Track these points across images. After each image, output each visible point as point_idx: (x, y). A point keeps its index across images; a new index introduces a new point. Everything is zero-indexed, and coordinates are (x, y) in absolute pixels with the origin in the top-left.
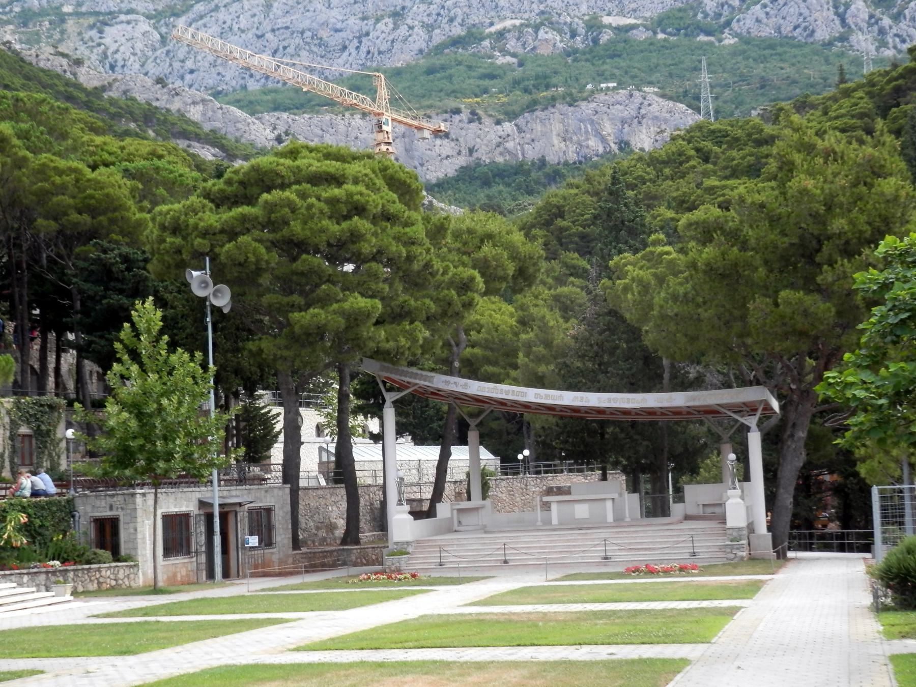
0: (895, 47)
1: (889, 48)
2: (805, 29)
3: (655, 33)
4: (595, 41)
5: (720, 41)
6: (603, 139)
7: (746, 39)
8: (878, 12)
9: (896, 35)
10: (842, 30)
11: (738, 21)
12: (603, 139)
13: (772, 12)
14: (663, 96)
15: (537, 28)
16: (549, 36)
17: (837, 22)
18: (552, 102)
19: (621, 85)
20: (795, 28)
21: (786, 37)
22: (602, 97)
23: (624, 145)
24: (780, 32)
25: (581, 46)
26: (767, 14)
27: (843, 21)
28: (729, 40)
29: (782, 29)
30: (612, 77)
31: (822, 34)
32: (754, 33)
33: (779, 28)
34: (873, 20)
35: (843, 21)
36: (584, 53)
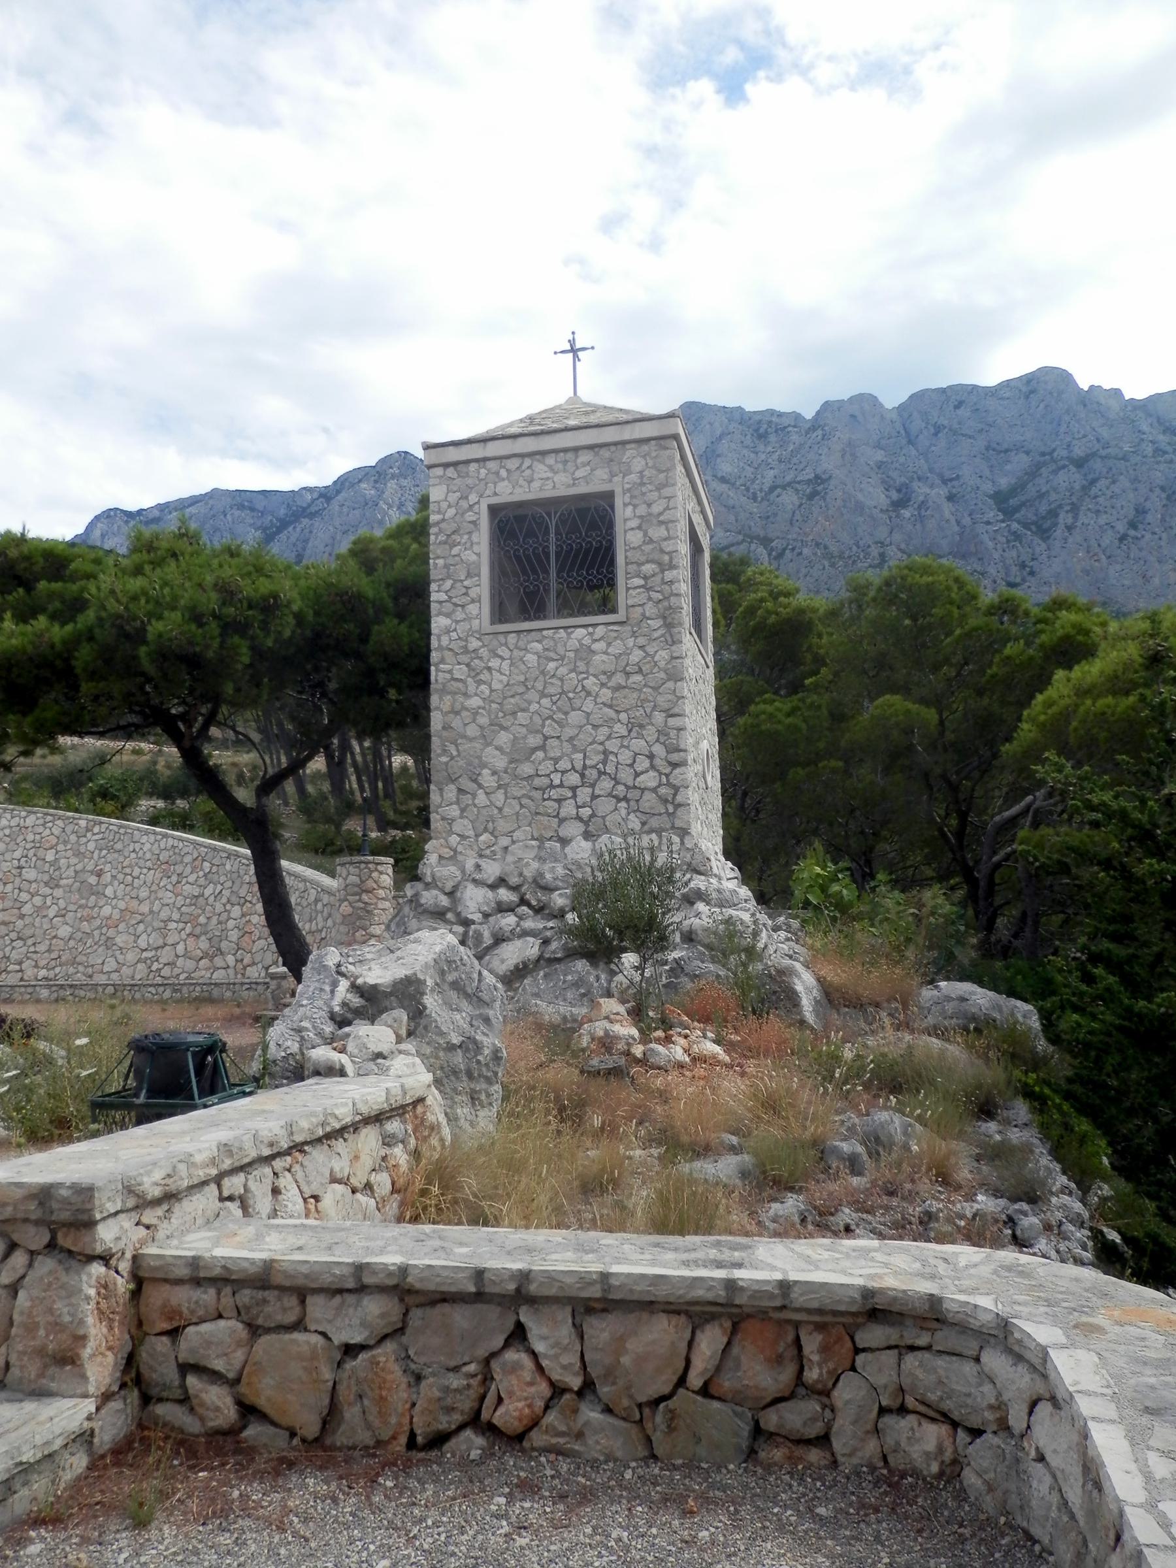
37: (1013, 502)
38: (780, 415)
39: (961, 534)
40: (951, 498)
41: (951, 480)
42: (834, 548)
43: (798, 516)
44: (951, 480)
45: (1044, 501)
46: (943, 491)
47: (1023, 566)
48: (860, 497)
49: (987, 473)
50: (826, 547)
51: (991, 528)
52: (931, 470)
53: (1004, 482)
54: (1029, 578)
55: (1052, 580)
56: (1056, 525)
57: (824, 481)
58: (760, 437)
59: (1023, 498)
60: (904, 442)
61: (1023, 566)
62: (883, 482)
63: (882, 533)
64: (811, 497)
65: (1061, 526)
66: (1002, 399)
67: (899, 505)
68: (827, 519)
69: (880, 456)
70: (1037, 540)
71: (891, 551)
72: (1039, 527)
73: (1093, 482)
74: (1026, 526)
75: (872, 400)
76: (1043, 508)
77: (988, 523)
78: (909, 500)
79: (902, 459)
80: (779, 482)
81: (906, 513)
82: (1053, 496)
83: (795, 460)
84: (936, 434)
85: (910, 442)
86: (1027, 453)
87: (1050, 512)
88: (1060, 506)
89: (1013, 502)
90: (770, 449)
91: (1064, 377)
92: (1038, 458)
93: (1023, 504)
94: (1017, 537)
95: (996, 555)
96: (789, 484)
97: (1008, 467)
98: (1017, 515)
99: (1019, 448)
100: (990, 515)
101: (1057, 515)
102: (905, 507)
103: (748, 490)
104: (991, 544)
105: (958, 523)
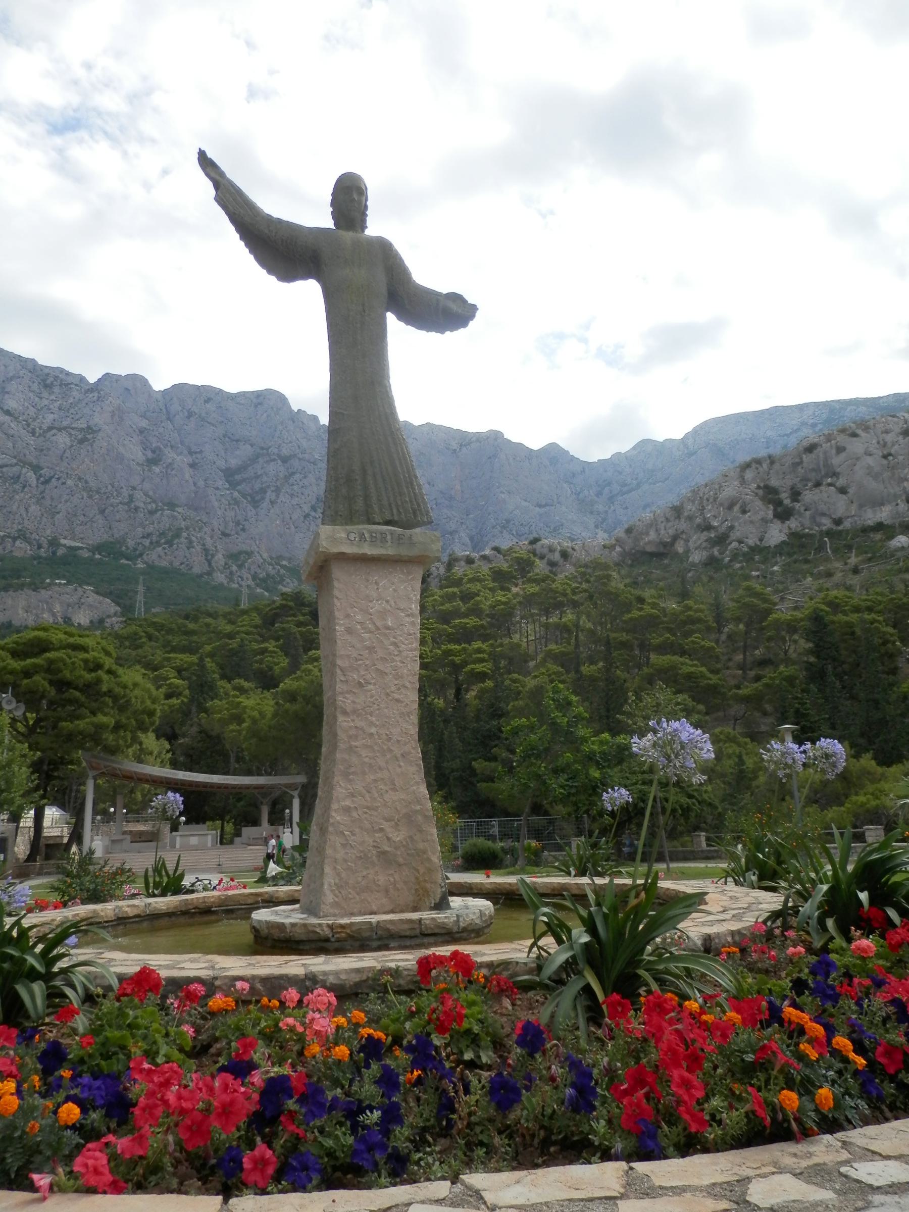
4: (54, 553)
6: (54, 615)
7: (151, 567)
8: (230, 562)
12: (54, 615)
14: (97, 593)
15: (15, 539)
16: (23, 545)
18: (21, 587)
19: (69, 583)
22: (57, 588)
23: (67, 620)
25: (44, 555)
27: (210, 564)
28: (141, 565)
30: (63, 577)
31: (197, 570)
32: (156, 563)
34: (226, 566)
35: (210, 564)
36: (46, 559)
37: (238, 477)
38: (68, 374)
39: (196, 493)
40: (192, 466)
42: (93, 484)
43: (68, 454)
46: (188, 459)
47: (238, 523)
48: (121, 450)
50: (86, 482)
52: (182, 443)
53: (234, 462)
56: (263, 498)
57: (94, 432)
58: (46, 386)
59: (245, 476)
60: (164, 417)
61: (238, 523)
62: (142, 443)
63: (136, 480)
64: (81, 442)
65: (267, 500)
68: (92, 461)
69: (144, 423)
70: (250, 507)
71: (138, 495)
73: (293, 474)
75: (143, 382)
76: (257, 486)
77: (217, 489)
78: (160, 460)
79: (161, 430)
80: (56, 425)
81: (157, 469)
82: (265, 479)
83: (72, 411)
84: (189, 417)
85: (169, 419)
86: (252, 446)
87: (261, 489)
88: (268, 487)
89: (238, 477)
90: (53, 397)
91: (281, 399)
93: (244, 480)
94: (237, 503)
96: (65, 428)
97: (238, 452)
98: (239, 487)
100: (220, 483)
101: (265, 492)
103: (28, 425)
104: (216, 504)
105: (195, 484)
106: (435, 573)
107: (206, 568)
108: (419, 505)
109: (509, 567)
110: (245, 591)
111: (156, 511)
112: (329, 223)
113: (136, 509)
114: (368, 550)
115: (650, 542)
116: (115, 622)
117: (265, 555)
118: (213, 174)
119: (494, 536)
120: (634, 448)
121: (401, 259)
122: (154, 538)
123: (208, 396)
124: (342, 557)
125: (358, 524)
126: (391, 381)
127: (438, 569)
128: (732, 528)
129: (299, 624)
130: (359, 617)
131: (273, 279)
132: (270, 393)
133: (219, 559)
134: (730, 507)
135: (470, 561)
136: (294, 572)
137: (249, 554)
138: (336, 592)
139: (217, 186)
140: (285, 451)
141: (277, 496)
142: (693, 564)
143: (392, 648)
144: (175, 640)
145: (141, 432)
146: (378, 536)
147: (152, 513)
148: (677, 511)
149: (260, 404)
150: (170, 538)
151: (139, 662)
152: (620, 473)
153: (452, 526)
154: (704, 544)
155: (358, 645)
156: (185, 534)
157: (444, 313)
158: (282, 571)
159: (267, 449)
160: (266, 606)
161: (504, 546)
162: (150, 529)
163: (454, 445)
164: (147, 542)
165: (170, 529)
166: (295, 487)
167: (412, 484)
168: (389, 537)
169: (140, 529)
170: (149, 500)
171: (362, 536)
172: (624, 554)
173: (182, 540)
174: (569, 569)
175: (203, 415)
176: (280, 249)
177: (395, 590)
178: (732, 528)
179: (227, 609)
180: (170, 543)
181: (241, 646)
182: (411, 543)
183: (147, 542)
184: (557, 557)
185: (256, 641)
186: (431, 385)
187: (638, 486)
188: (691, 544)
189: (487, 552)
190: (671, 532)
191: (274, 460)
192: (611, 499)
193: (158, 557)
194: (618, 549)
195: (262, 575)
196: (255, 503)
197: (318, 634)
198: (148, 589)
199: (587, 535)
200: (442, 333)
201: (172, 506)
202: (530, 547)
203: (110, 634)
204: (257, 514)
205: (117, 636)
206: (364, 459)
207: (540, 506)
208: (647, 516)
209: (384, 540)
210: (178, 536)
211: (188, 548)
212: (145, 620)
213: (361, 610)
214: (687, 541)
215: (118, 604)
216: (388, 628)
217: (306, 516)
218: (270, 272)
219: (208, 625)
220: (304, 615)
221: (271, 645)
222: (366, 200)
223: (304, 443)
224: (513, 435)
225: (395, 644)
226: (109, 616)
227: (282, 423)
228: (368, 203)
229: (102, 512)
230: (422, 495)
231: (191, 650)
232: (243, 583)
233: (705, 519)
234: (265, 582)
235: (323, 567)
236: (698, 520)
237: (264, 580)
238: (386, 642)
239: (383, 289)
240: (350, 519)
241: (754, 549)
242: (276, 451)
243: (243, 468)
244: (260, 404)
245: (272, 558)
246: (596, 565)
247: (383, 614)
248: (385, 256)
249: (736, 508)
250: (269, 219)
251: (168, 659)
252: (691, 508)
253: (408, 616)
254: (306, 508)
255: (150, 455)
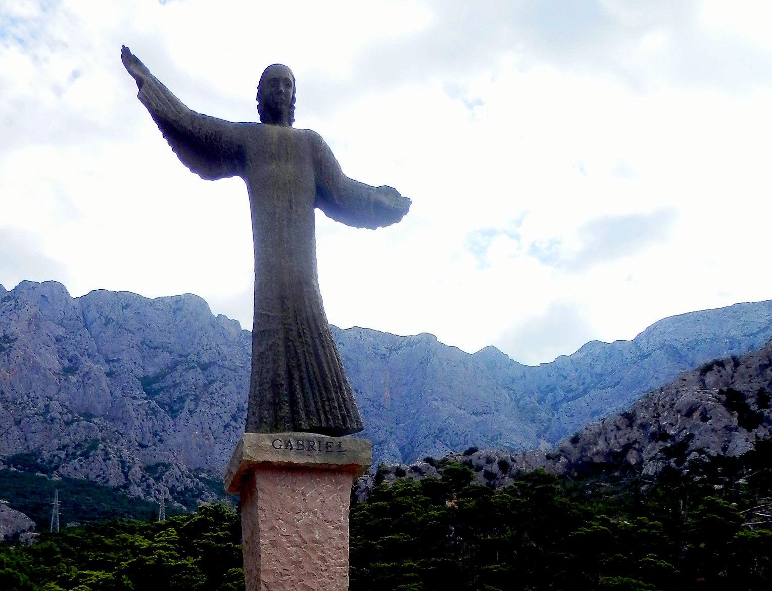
0: (155, 497)
1: (151, 497)
2: (104, 478)
3: (9, 467)
5: (51, 478)
7: (67, 479)
8: (147, 475)
9: (157, 490)
10: (125, 482)
11: (63, 467)
13: (84, 465)
14: (11, 506)
17: (123, 477)
20: (98, 477)
21: (92, 481)
24: (88, 478)
26: (81, 465)
27: (126, 478)
28: (56, 478)
29: (90, 476)
31: (113, 483)
32: (72, 476)
33: (88, 475)
34: (144, 479)
35: (126, 478)
37: (155, 386)
39: (113, 403)
40: (108, 374)
41: (113, 361)
44: (113, 361)
45: (177, 390)
46: (106, 368)
48: (38, 359)
49: (140, 361)
51: (135, 402)
52: (99, 351)
53: (152, 371)
54: (158, 444)
55: (175, 448)
56: (182, 408)
59: (163, 385)
60: (82, 325)
61: (155, 434)
62: (59, 351)
63: (52, 390)
66: (158, 309)
67: (69, 371)
68: (8, 371)
69: (61, 332)
71: (55, 405)
72: (171, 408)
74: (162, 405)
75: (61, 288)
76: (175, 396)
77: (135, 398)
78: (77, 369)
79: (78, 338)
81: (73, 379)
82: (183, 387)
84: (106, 325)
85: (86, 326)
86: (170, 353)
87: (180, 398)
88: (187, 395)
89: (155, 386)
92: (177, 358)
93: (162, 389)
94: (155, 412)
95: (137, 423)
97: (155, 360)
98: (157, 397)
99: (164, 348)
101: (184, 401)
102: (73, 374)
105: (111, 393)
106: (363, 486)
107: (123, 481)
108: (348, 412)
109: (443, 480)
110: (163, 505)
111: (72, 422)
112: (255, 118)
113: (53, 419)
114: (295, 459)
115: (598, 453)
116: (29, 537)
117: (183, 467)
118: (136, 72)
119: (426, 447)
120: (580, 350)
121: (330, 152)
122: (70, 450)
123: (127, 302)
124: (267, 467)
125: (284, 431)
126: (319, 280)
127: (365, 481)
128: (691, 437)
129: (218, 539)
130: (284, 530)
131: (196, 176)
132: (190, 297)
133: (136, 472)
134: (689, 413)
135: (399, 473)
136: (214, 485)
137: (167, 466)
138: (260, 503)
139: (140, 83)
140: (205, 359)
141: (197, 405)
142: (648, 477)
143: (319, 562)
144: (91, 556)
145: (58, 340)
146: (305, 444)
147: (67, 424)
148: (629, 418)
149: (178, 309)
150: (85, 449)
151: (54, 579)
152: (565, 378)
153: (381, 436)
154: (660, 455)
155: (284, 560)
156: (101, 446)
157: (375, 207)
158: (201, 484)
159: (186, 356)
160: (184, 521)
161: (438, 457)
162: (66, 441)
163: (383, 350)
164: (63, 454)
165: (86, 440)
166: (215, 396)
167: (341, 389)
168: (316, 445)
169: (56, 441)
170: (66, 411)
171: (288, 444)
172: (569, 466)
173: (99, 451)
174: (509, 482)
175: (121, 322)
176: (202, 145)
177: (323, 501)
178: (691, 437)
179: (144, 524)
180: (86, 455)
181: (159, 560)
182: (341, 452)
183: (63, 454)
184: (495, 468)
185: (172, 557)
186: (361, 284)
187: (585, 391)
188: (645, 455)
189: (419, 463)
190: (623, 441)
191: (193, 367)
192: (555, 406)
193: (75, 469)
194: (563, 460)
195: (181, 488)
196: (174, 413)
197: (240, 551)
198: (64, 503)
199: (526, 443)
200: (374, 229)
201: (88, 416)
202: (465, 458)
203: (24, 550)
204: (175, 425)
205: (30, 551)
206: (296, 362)
207: (476, 414)
208: (595, 423)
209: (311, 448)
210: (94, 447)
211: (105, 460)
212: (60, 534)
213: (287, 522)
214: (640, 451)
215: (33, 518)
216: (315, 542)
217: (226, 426)
218: (193, 169)
219: (125, 540)
220: (222, 530)
221: (189, 561)
222: (294, 92)
223: (225, 350)
224: (446, 338)
225: (323, 559)
226: (23, 531)
227: (201, 329)
228: (296, 95)
229: (18, 423)
230: (351, 400)
231: (108, 567)
232: (160, 497)
233: (660, 427)
234: (186, 496)
235: (246, 480)
236: (653, 429)
237: (181, 493)
238: (313, 557)
239: (311, 184)
240: (275, 426)
241: (718, 460)
242: (195, 358)
243: (159, 377)
244: (178, 309)
245: (190, 471)
246: (537, 477)
247: (310, 526)
248: (314, 151)
249: (696, 415)
250: (193, 116)
251: (84, 576)
252: (643, 415)
253: (337, 528)
254: (227, 418)
255: (66, 364)
